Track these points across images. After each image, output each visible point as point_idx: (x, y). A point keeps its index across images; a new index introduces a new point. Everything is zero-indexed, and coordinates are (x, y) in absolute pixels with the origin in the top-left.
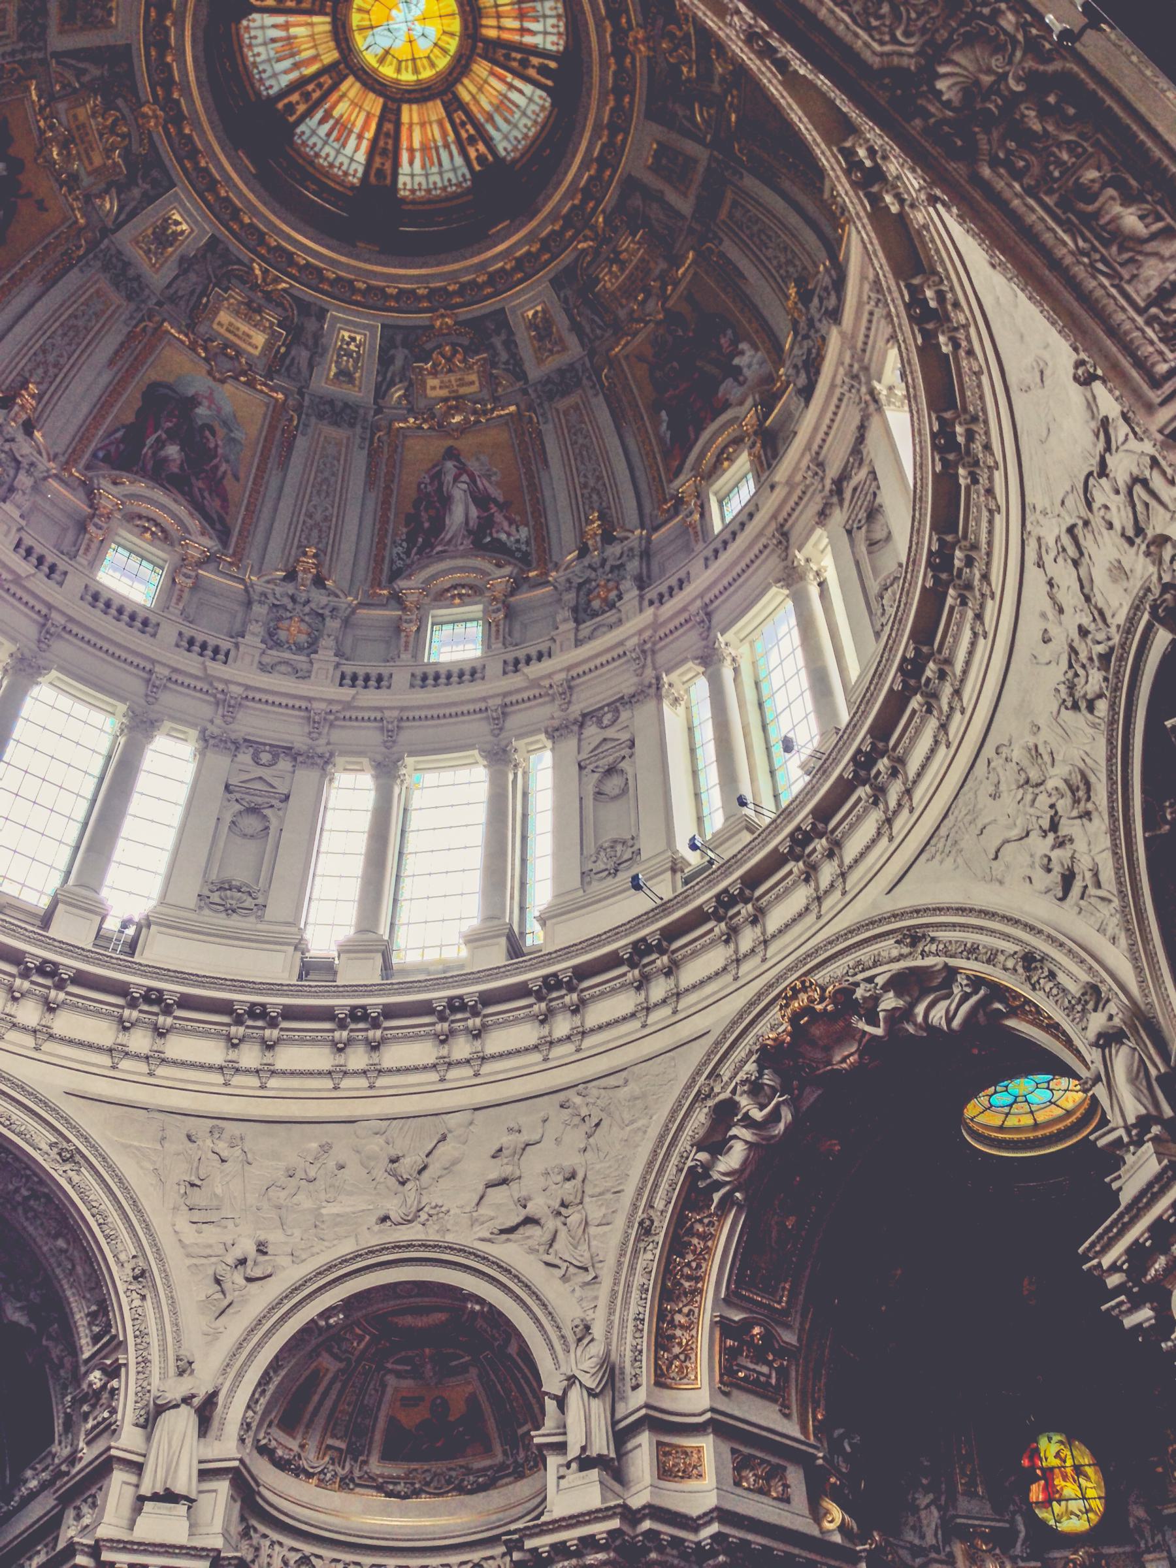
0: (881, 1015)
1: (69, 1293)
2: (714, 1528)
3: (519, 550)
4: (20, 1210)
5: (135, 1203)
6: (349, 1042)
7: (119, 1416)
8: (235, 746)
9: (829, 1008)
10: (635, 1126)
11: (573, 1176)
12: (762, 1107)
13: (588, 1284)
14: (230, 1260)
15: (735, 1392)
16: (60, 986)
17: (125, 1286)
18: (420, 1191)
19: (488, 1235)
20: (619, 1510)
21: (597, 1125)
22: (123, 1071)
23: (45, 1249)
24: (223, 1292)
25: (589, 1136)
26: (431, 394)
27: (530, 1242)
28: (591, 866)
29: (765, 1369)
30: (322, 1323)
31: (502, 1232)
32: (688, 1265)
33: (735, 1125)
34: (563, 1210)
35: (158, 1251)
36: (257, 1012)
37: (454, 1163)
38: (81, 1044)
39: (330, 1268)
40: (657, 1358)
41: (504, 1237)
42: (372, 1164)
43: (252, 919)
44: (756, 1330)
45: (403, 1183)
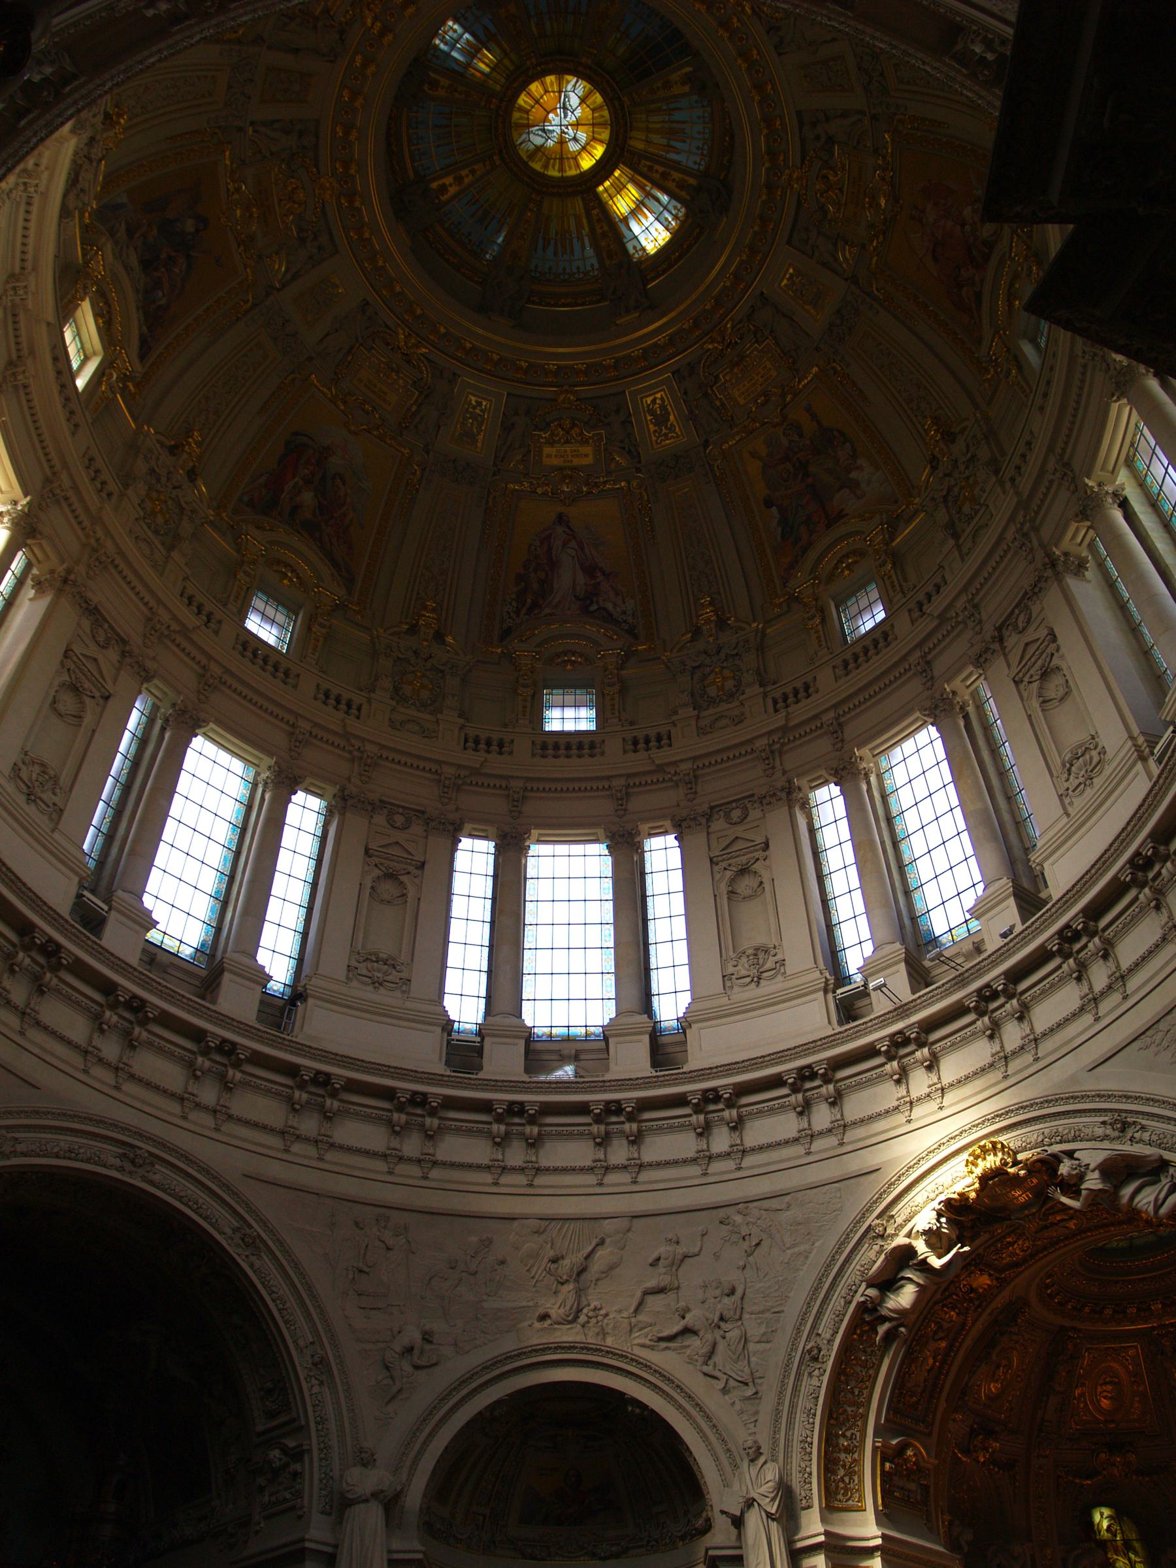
0: (1084, 1192)
3: (625, 621)
5: (310, 1288)
6: (507, 1137)
7: (306, 1503)
8: (372, 807)
9: (1022, 1172)
10: (796, 1250)
13: (748, 1398)
14: (398, 1349)
16: (237, 1065)
18: (580, 1292)
21: (758, 1245)
22: (296, 1154)
24: (392, 1378)
26: (547, 461)
27: (688, 1351)
28: (731, 970)
29: (912, 1486)
31: (661, 1339)
33: (908, 1266)
34: (722, 1324)
36: (419, 1100)
37: (612, 1268)
38: (256, 1125)
39: (496, 1362)
41: (663, 1345)
42: (531, 1262)
43: (398, 994)
44: (910, 1453)
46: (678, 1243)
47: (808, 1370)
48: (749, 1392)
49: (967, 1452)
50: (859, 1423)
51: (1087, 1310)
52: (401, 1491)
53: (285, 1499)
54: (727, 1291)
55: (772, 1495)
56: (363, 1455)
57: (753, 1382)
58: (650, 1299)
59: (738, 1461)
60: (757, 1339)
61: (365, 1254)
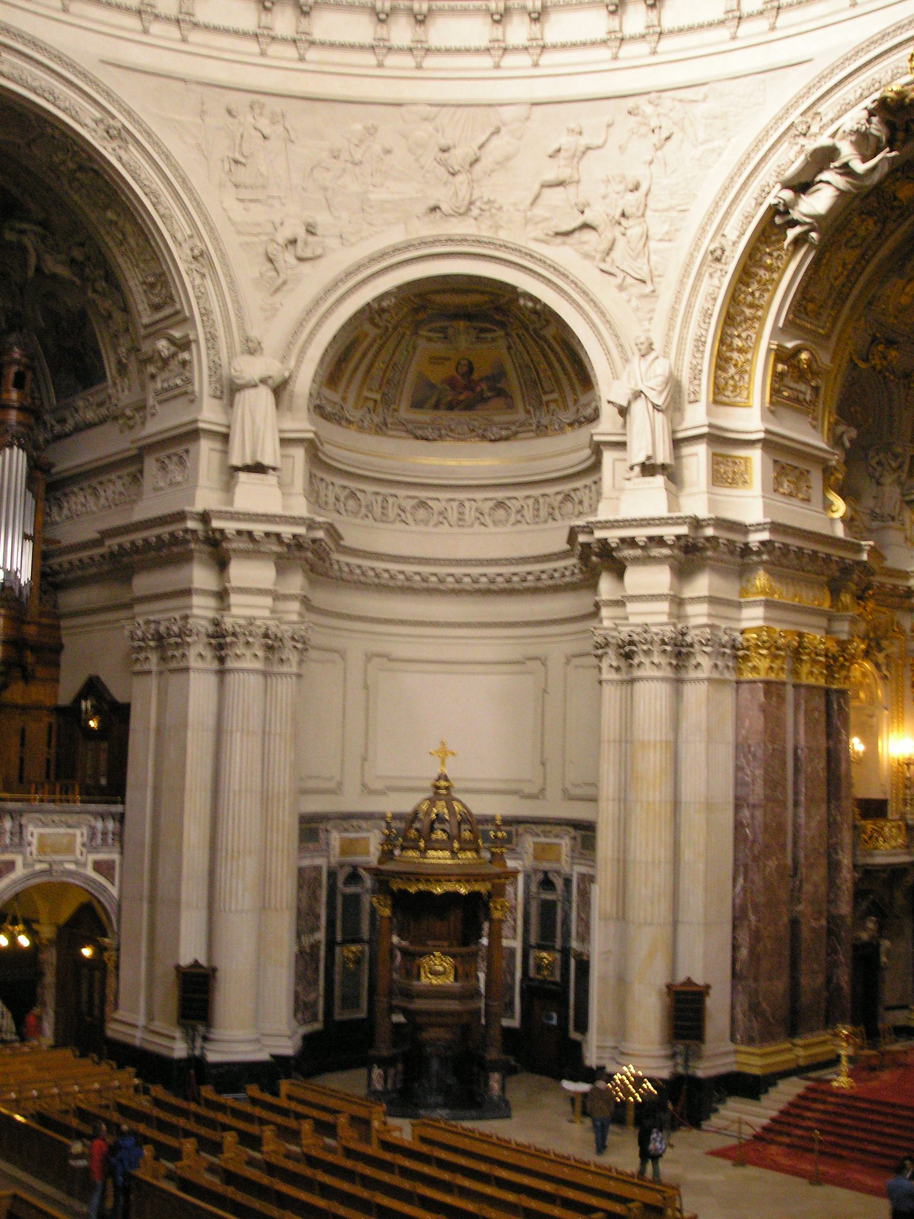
1: (120, 260)
2: (765, 536)
4: (65, 181)
5: (184, 181)
7: (196, 388)
11: (636, 188)
12: (865, 160)
13: (646, 296)
14: (281, 241)
15: (781, 410)
17: (186, 266)
19: (542, 236)
20: (688, 520)
21: (668, 138)
23: (93, 217)
25: (658, 148)
29: (802, 387)
30: (375, 306)
32: (752, 294)
34: (623, 221)
35: (212, 230)
37: (508, 158)
39: (383, 255)
40: (716, 378)
41: (559, 240)
44: (804, 356)
45: (453, 175)
46: (580, 133)
47: (710, 270)
48: (648, 288)
49: (866, 360)
50: (757, 325)
52: (290, 377)
53: (177, 386)
54: (631, 186)
55: (659, 389)
56: (250, 344)
57: (652, 281)
58: (547, 192)
59: (629, 354)
60: (659, 237)
61: (241, 145)
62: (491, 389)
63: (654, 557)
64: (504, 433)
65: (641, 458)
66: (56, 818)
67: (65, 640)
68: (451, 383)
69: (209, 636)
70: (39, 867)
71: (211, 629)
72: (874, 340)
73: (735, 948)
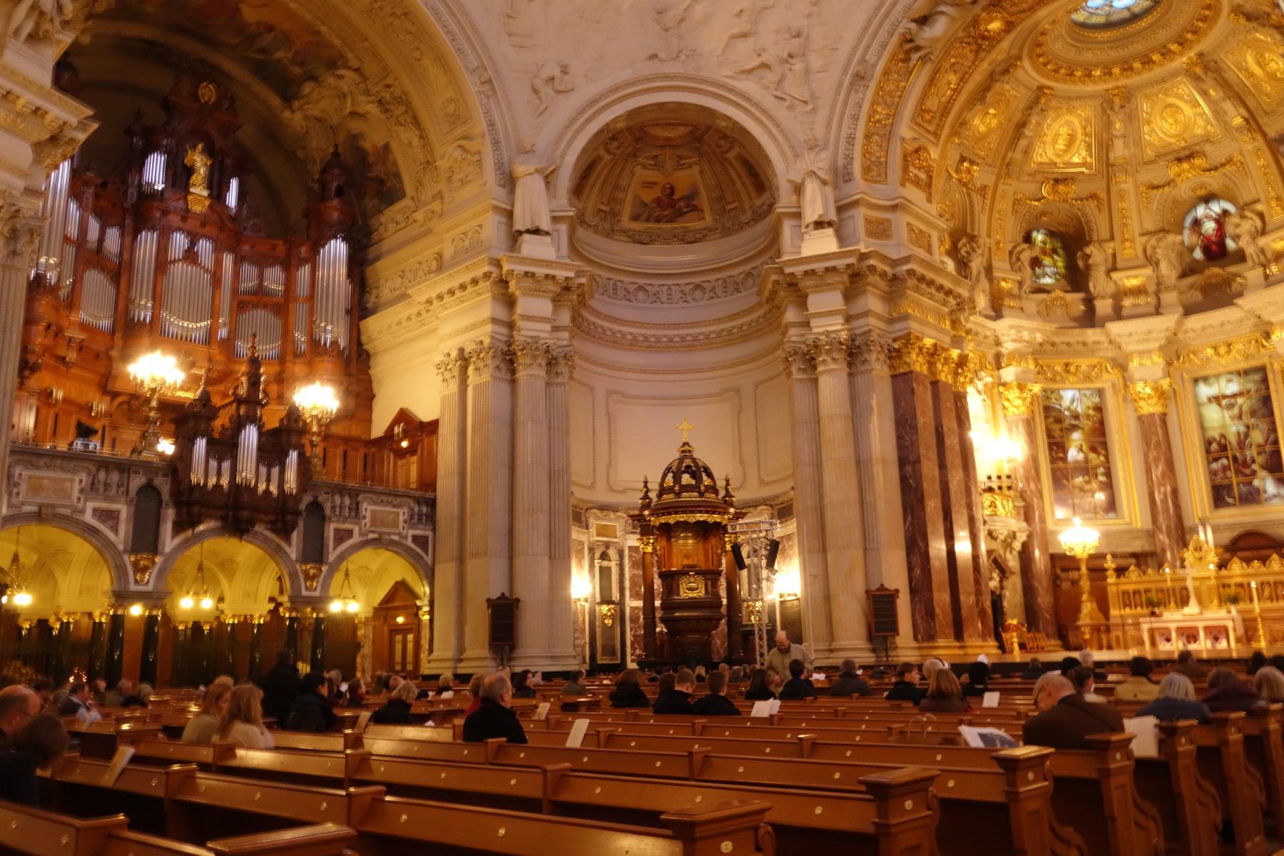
11: (798, 35)
19: (730, 73)
24: (539, 98)
34: (790, 60)
48: (809, 108)
51: (1062, 71)
62: (688, 206)
63: (829, 284)
64: (698, 236)
65: (815, 218)
66: (385, 498)
67: (375, 391)
68: (658, 202)
69: (504, 354)
70: (371, 536)
71: (506, 349)
72: (963, 159)
73: (910, 570)
